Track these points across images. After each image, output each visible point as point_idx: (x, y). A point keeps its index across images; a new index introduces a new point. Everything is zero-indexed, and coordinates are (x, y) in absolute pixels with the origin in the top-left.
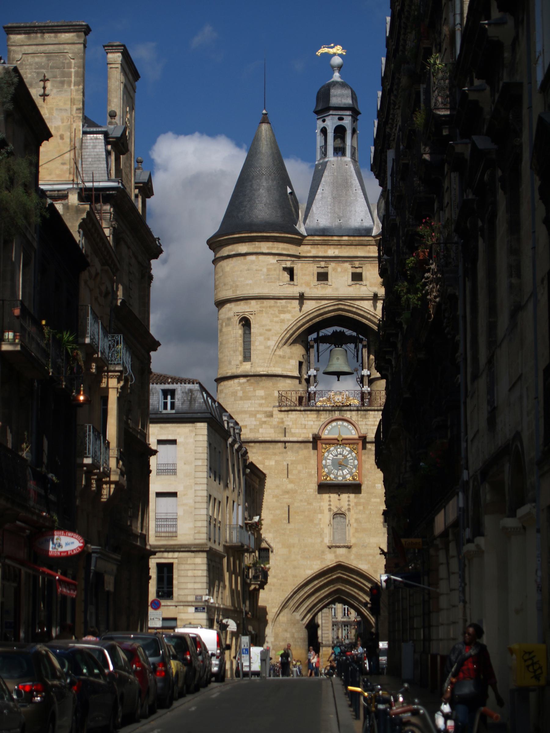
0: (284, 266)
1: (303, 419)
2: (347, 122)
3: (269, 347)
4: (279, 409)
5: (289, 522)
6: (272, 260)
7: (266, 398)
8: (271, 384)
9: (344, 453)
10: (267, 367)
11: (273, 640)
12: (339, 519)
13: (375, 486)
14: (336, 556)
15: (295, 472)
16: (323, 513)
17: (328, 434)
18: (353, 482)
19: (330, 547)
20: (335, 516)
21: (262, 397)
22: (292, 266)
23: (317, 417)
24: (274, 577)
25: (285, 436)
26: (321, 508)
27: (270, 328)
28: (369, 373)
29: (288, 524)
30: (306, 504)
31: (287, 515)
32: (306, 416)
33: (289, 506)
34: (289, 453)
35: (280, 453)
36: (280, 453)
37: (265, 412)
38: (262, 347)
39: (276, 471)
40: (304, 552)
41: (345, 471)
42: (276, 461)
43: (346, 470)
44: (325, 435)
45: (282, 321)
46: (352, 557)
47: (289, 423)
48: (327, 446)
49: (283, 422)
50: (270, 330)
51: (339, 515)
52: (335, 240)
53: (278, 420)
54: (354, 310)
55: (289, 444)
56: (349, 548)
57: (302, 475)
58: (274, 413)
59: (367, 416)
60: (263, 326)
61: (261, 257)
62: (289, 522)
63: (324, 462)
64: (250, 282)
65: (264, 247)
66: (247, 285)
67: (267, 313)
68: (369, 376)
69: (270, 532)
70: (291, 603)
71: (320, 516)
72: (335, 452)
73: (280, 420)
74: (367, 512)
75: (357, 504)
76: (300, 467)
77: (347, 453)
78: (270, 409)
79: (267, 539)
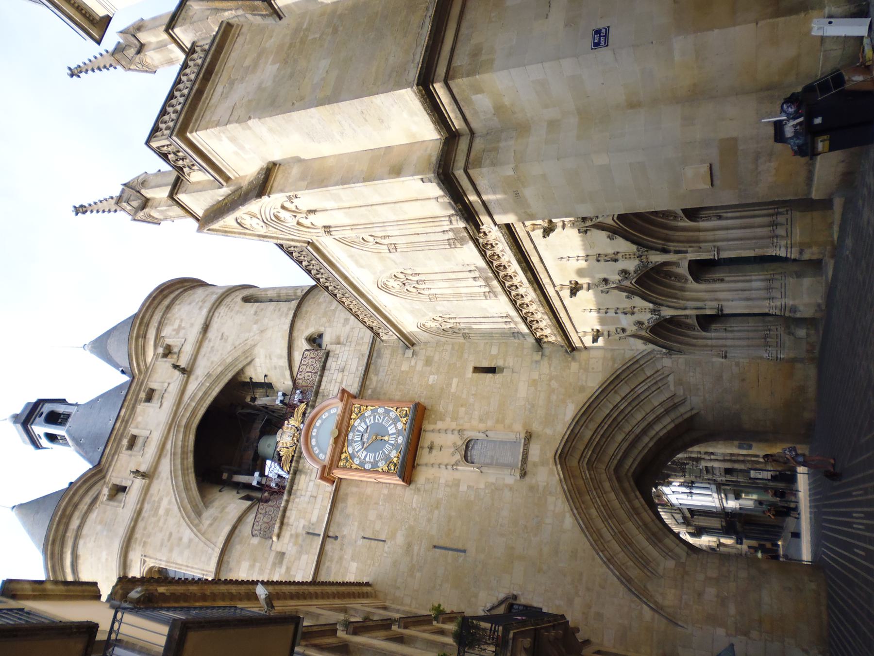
0: (105, 498)
1: (302, 498)
2: (47, 408)
3: (190, 541)
4: (275, 539)
5: (464, 551)
6: (93, 516)
7: (255, 560)
8: (238, 547)
9: (362, 430)
10: (213, 550)
11: (721, 632)
12: (475, 453)
13: (431, 386)
14: (543, 463)
15: (378, 526)
16: (459, 481)
17: (325, 454)
18: (410, 416)
19: (524, 474)
20: (469, 458)
21: (250, 566)
22: (110, 485)
23: (306, 473)
24: (570, 602)
25: (319, 535)
26: (450, 483)
27: (168, 533)
28: (280, 394)
29: (468, 554)
30: (436, 512)
31: (450, 552)
32: (298, 493)
33: (435, 547)
34: (345, 531)
35: (341, 549)
36: (341, 549)
37: (274, 564)
38: (186, 553)
39: (369, 562)
40: (526, 527)
41: (392, 430)
42: (353, 559)
43: (389, 429)
44: (325, 457)
45: (167, 512)
46: (549, 431)
47: (301, 526)
48: (343, 456)
49: (297, 536)
50: (171, 534)
51: (467, 451)
52: (121, 425)
53: (291, 544)
54: (193, 404)
55: (331, 529)
56: (531, 436)
57: (385, 514)
58: (279, 549)
59: (326, 394)
60: (162, 545)
61: (85, 531)
62: (464, 551)
63: (368, 466)
64: (104, 554)
65: (75, 523)
66: (107, 559)
67: (149, 536)
68: (284, 395)
69: (476, 596)
70: (634, 573)
71: (463, 488)
72: (357, 446)
73: (293, 540)
74: (471, 400)
75: (455, 418)
76: (372, 515)
77: (363, 424)
78: (273, 554)
79: (489, 606)
